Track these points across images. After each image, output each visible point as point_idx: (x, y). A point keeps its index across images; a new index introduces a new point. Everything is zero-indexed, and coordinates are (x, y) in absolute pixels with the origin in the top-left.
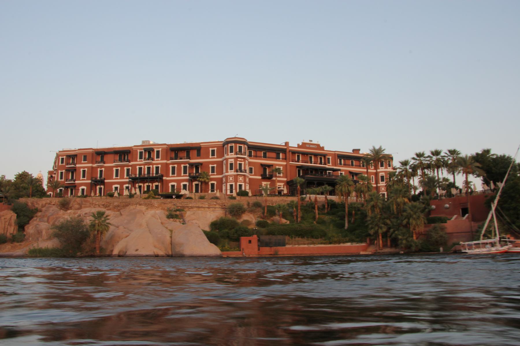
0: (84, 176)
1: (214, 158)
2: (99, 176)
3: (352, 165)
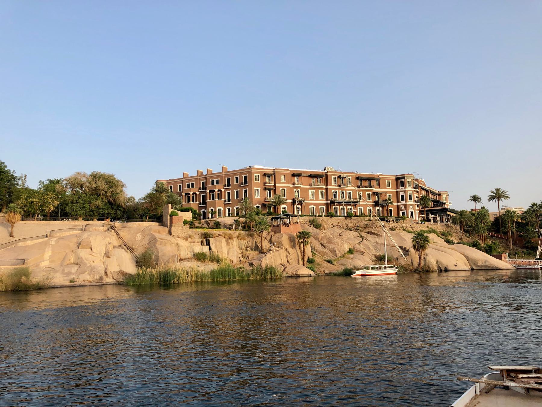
1: (390, 189)
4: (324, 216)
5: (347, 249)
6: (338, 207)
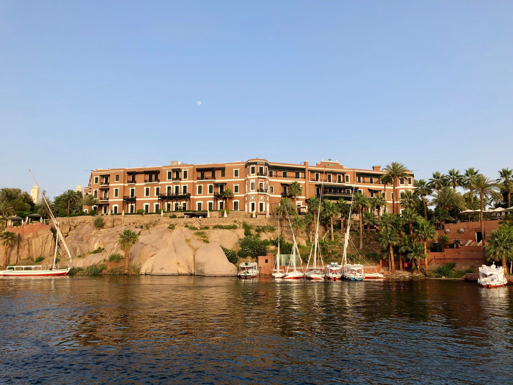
0: (116, 195)
1: (238, 178)
2: (130, 195)
3: (371, 182)
4: (123, 214)
5: (96, 248)
6: (171, 203)
